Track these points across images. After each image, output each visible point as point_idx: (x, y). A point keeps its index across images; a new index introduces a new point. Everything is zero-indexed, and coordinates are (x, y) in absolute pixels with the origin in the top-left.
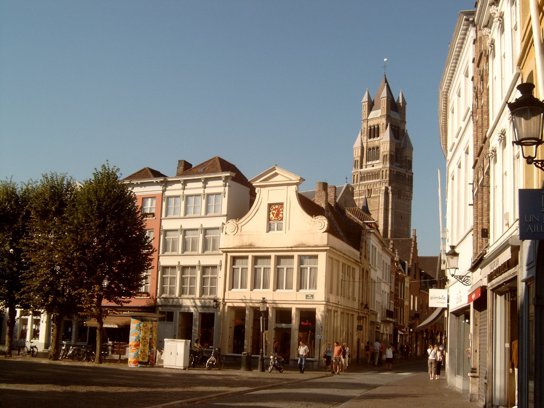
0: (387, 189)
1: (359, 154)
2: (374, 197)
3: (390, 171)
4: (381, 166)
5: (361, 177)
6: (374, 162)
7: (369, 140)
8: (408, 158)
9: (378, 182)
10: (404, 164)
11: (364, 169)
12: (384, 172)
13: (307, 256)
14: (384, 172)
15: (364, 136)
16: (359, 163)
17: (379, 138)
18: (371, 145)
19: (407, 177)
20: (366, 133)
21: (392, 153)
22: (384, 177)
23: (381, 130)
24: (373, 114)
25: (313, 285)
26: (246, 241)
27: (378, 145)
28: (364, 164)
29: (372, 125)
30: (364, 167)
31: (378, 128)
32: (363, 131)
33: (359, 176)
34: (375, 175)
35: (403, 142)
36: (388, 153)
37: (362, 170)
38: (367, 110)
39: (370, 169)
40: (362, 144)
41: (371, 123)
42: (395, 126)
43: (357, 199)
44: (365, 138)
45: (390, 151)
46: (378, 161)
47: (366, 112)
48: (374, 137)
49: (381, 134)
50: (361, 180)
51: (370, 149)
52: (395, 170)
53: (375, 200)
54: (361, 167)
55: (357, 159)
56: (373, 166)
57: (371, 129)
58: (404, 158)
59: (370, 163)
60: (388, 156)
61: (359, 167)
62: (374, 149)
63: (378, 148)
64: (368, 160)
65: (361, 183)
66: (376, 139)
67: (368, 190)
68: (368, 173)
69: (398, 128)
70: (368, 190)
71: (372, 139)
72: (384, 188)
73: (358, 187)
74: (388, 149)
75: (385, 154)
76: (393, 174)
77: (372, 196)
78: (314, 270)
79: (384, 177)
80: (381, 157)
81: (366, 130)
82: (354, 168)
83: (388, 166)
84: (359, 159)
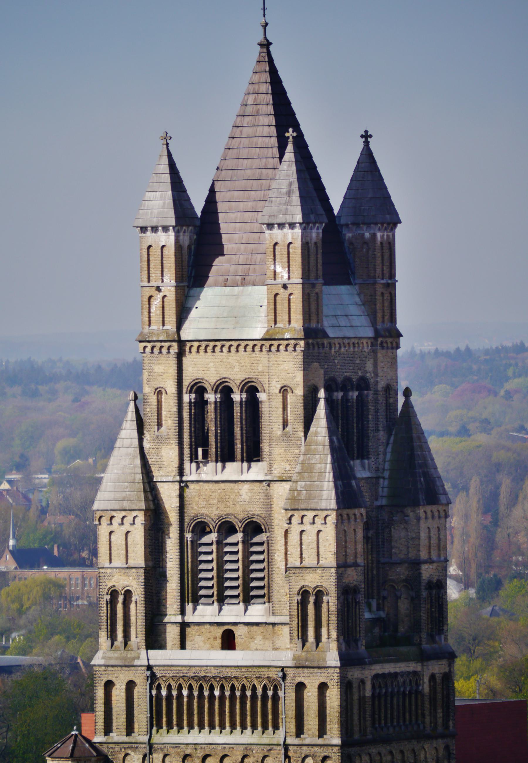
1: (138, 557)
3: (346, 686)
5: (155, 703)
7: (191, 473)
8: (427, 572)
9: (271, 746)
10: (404, 606)
12: (311, 696)
15: (159, 440)
17: (257, 471)
18: (206, 505)
19: (426, 688)
20: (170, 422)
21: (353, 576)
22: (311, 722)
27: (256, 511)
28: (172, 615)
29: (211, 378)
30: (172, 634)
31: (253, 406)
33: (141, 692)
36: (328, 581)
37: (157, 657)
38: (170, 279)
39: (204, 655)
41: (202, 368)
42: (346, 385)
45: (342, 566)
46: (257, 612)
48: (226, 456)
51: (201, 528)
54: (154, 639)
57: (200, 404)
59: (206, 612)
60: (331, 602)
61: (138, 636)
62: (227, 528)
64: (191, 595)
65: (165, 737)
66: (233, 470)
69: (363, 384)
74: (329, 558)
75: (311, 580)
76: (362, 699)
79: (311, 722)
81: (169, 405)
83: (332, 658)
84: (135, 584)
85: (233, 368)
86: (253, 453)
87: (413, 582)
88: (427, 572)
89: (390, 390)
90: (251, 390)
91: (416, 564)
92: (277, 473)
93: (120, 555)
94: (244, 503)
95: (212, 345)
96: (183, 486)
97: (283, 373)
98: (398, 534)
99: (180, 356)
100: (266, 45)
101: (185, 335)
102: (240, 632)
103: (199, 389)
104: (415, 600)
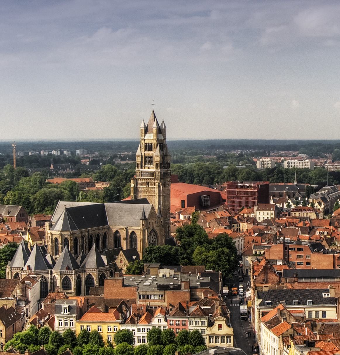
0: (159, 183)
1: (140, 160)
2: (151, 188)
3: (160, 173)
4: (154, 170)
5: (141, 174)
6: (149, 166)
8: (168, 162)
10: (166, 165)
11: (143, 170)
12: (157, 174)
13: (229, 336)
14: (157, 174)
15: (142, 149)
16: (140, 165)
17: (152, 152)
18: (147, 155)
20: (143, 147)
21: (161, 162)
22: (157, 176)
23: (153, 147)
24: (148, 136)
25: (230, 342)
26: (213, 332)
27: (152, 156)
28: (143, 166)
29: (147, 143)
31: (151, 145)
32: (141, 146)
33: (140, 173)
34: (151, 174)
35: (165, 152)
36: (159, 163)
38: (143, 133)
39: (146, 170)
40: (141, 153)
41: (146, 141)
43: (139, 187)
44: (143, 150)
45: (160, 161)
46: (152, 166)
47: (143, 134)
48: (149, 150)
49: (154, 150)
50: (141, 176)
51: (146, 157)
52: (162, 172)
53: (152, 189)
55: (138, 162)
56: (149, 168)
57: (146, 145)
58: (166, 162)
59: (146, 166)
60: (159, 165)
62: (149, 157)
63: (152, 157)
64: (145, 164)
65: (142, 177)
66: (149, 152)
67: (147, 182)
68: (146, 172)
69: (162, 143)
70: (147, 182)
71: (147, 152)
72: (157, 184)
73: (140, 180)
74: (159, 161)
75: (157, 162)
77: (149, 186)
78: (230, 339)
79: (157, 176)
80: (154, 163)
81: (143, 145)
82: (136, 168)
83: (159, 170)
84: (140, 163)
85: (150, 142)
86: (151, 150)
87: (167, 163)
88: (168, 162)
89: (165, 144)
90: (151, 144)
91: (167, 161)
92: (154, 151)
93: (138, 160)
94: (151, 155)
95: (147, 139)
96: (145, 153)
97: (155, 142)
98: (166, 158)
99: (144, 141)
100: (153, 110)
101: (145, 138)
102: (150, 168)
103: (146, 143)
104: (167, 165)
